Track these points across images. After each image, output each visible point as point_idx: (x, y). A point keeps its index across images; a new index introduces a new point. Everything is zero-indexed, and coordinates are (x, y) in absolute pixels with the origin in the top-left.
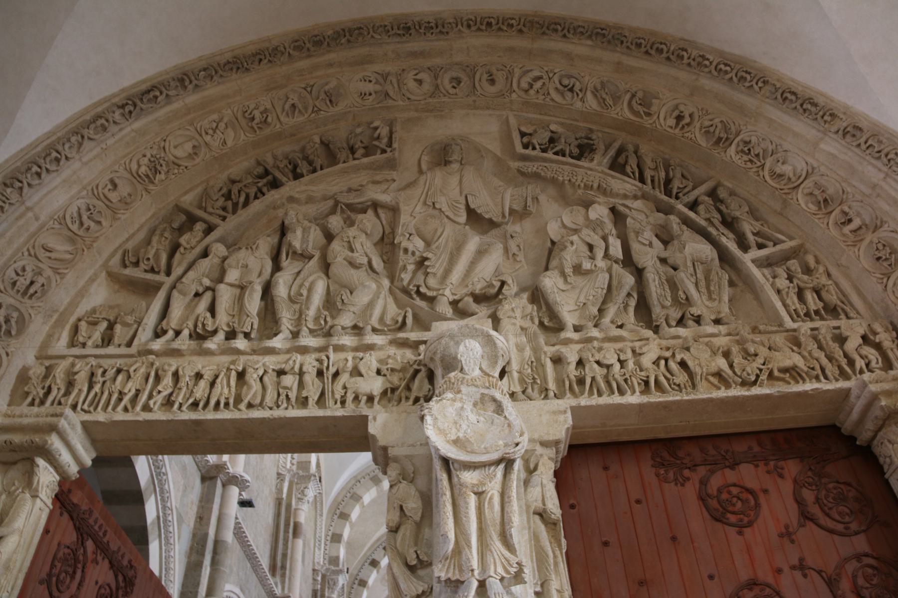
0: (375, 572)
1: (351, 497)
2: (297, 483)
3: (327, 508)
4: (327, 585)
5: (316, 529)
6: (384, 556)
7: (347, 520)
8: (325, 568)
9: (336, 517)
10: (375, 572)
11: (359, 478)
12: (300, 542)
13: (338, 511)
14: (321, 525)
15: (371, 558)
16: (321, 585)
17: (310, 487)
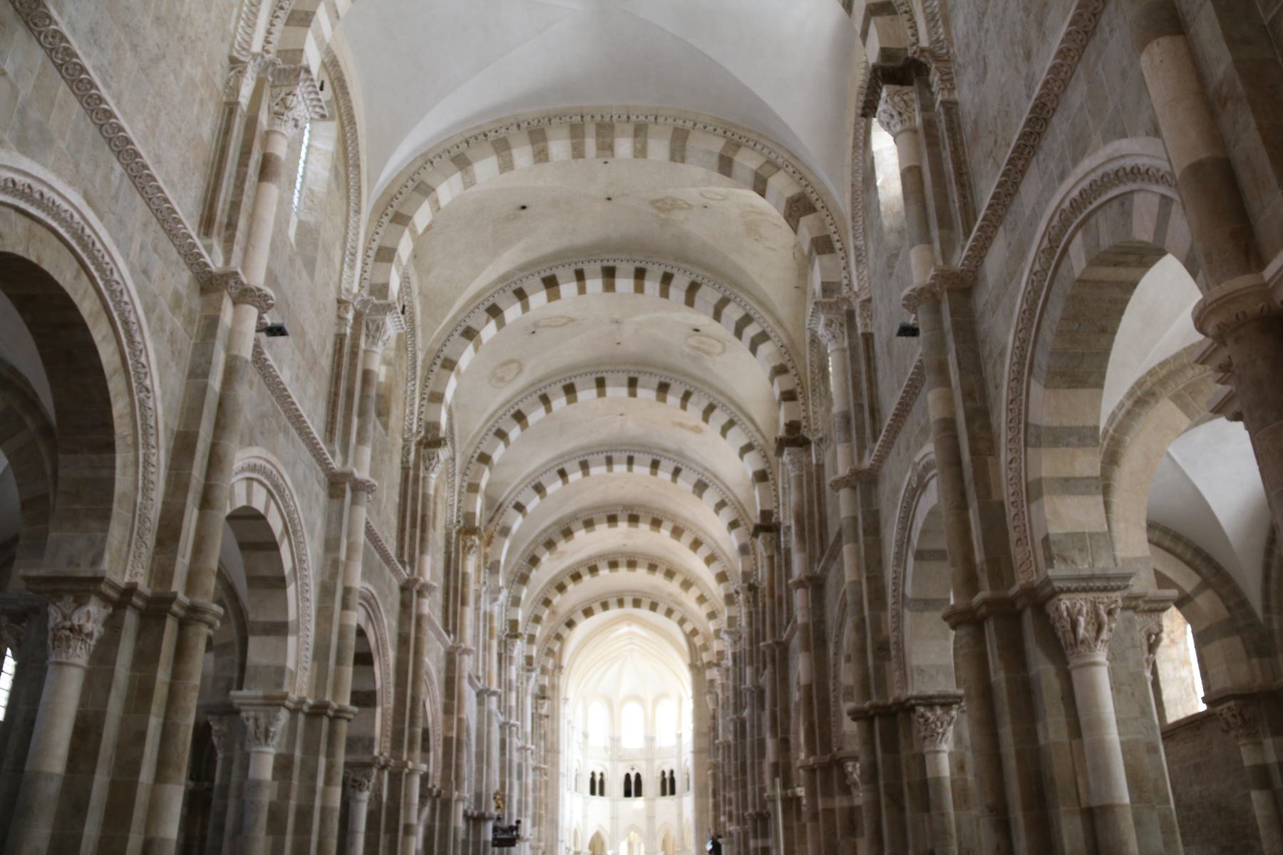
0: (471, 347)
1: (416, 189)
2: (273, 86)
3: (373, 202)
4: (364, 331)
5: (347, 233)
6: (487, 322)
7: (406, 225)
8: (359, 298)
9: (385, 220)
10: (471, 347)
11: (430, 156)
12: (272, 191)
13: (390, 209)
14: (357, 228)
15: (463, 324)
16: (352, 328)
17: (298, 92)
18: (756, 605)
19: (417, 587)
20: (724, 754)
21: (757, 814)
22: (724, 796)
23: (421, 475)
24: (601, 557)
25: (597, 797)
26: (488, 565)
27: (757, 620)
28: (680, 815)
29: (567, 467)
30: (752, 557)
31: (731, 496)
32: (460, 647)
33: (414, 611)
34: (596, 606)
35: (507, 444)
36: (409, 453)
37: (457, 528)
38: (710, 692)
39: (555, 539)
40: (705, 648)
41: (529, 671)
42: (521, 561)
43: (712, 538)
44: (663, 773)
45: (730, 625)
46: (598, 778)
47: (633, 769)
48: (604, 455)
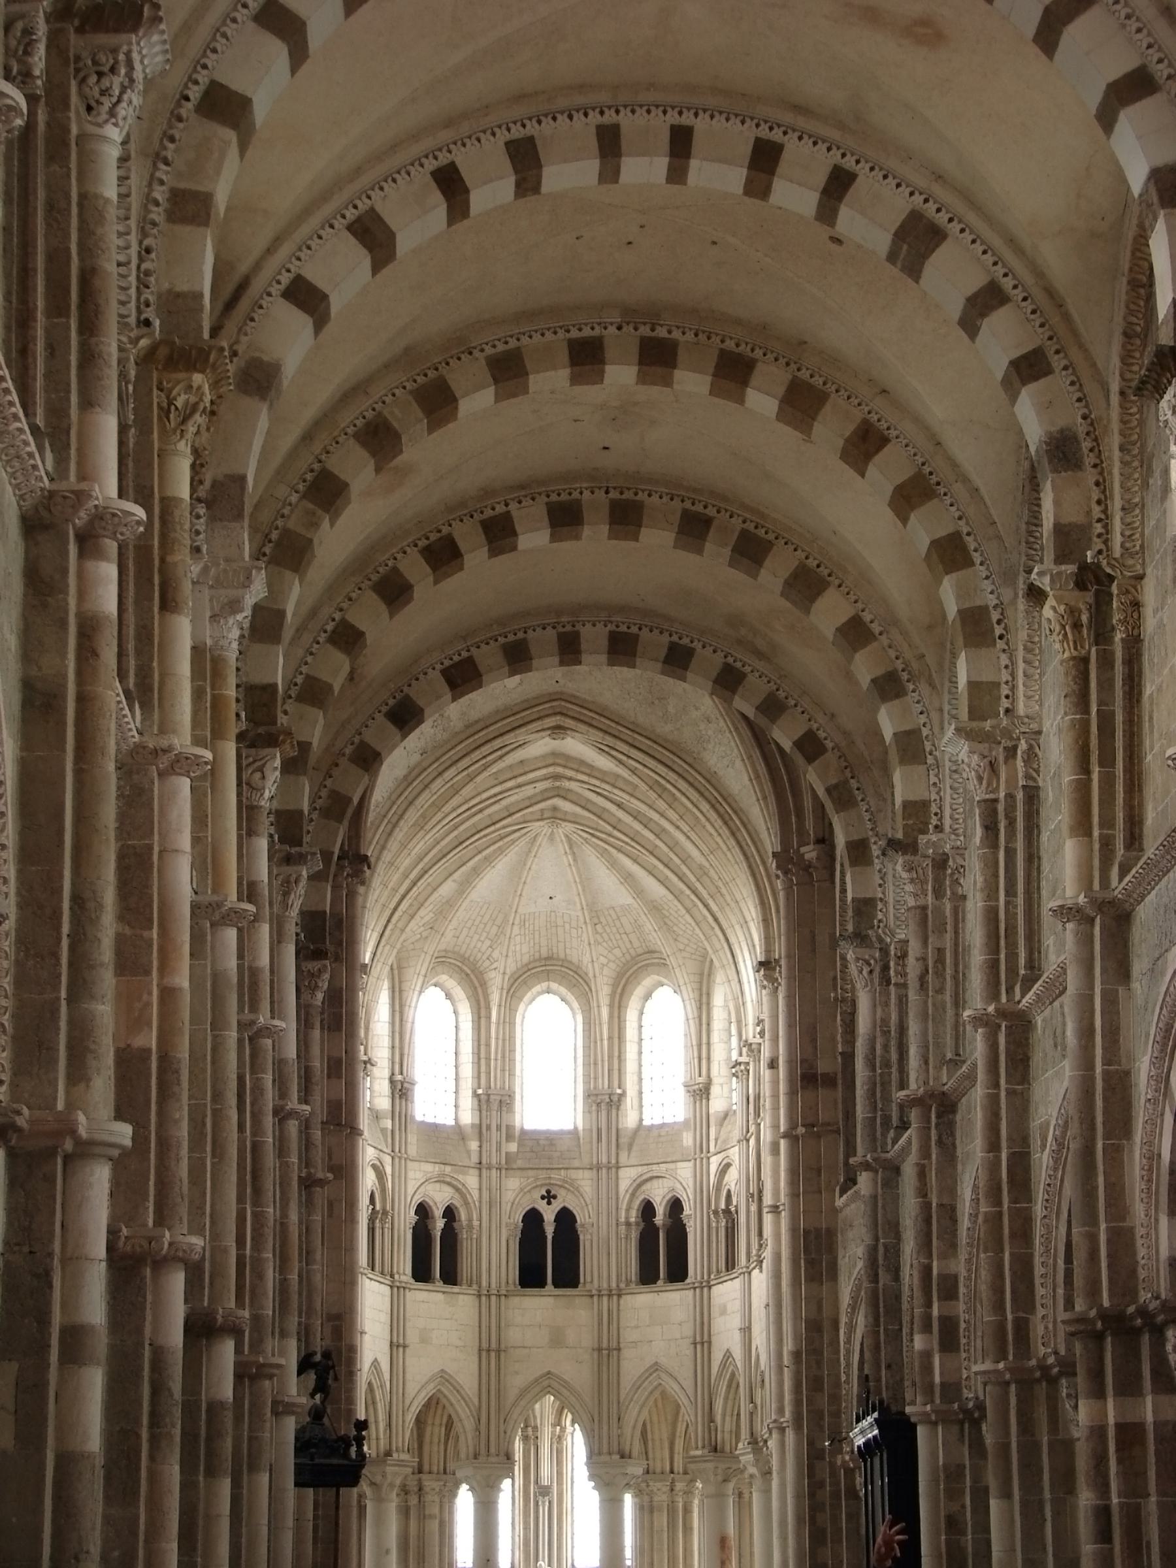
18: (1102, 635)
19: (81, 518)
20: (925, 1130)
21: (1104, 1315)
22: (927, 1271)
23: (74, 130)
24: (525, 489)
25: (439, 1284)
26: (202, 492)
27: (1106, 685)
28: (703, 1341)
29: (464, 160)
30: (1090, 476)
31: (1028, 279)
32: (164, 751)
33: (72, 602)
34: (488, 656)
35: (299, 54)
36: (26, 53)
37: (144, 343)
38: (860, 938)
39: (395, 416)
40: (843, 797)
41: (288, 860)
42: (282, 491)
43: (917, 420)
44: (648, 1209)
45: (975, 713)
46: (440, 1224)
47: (549, 1197)
48: (595, 118)
